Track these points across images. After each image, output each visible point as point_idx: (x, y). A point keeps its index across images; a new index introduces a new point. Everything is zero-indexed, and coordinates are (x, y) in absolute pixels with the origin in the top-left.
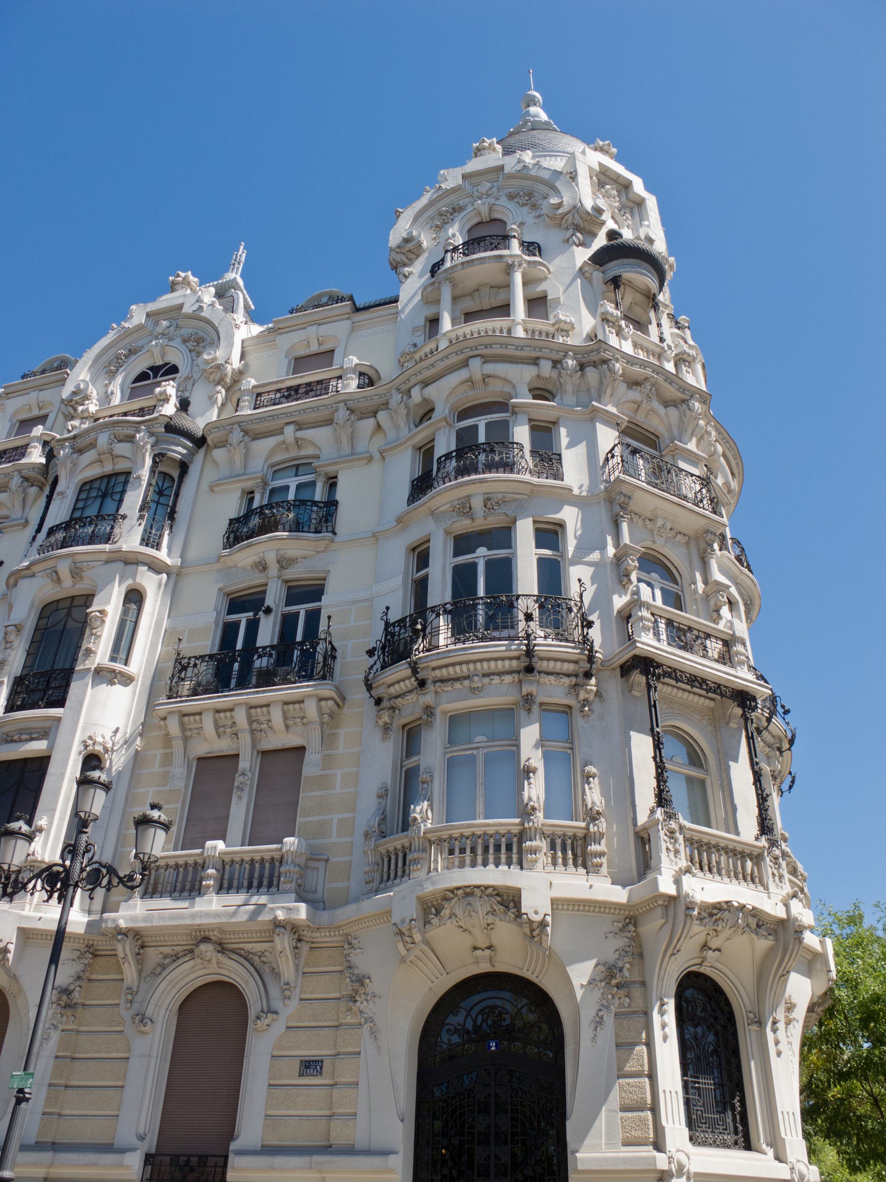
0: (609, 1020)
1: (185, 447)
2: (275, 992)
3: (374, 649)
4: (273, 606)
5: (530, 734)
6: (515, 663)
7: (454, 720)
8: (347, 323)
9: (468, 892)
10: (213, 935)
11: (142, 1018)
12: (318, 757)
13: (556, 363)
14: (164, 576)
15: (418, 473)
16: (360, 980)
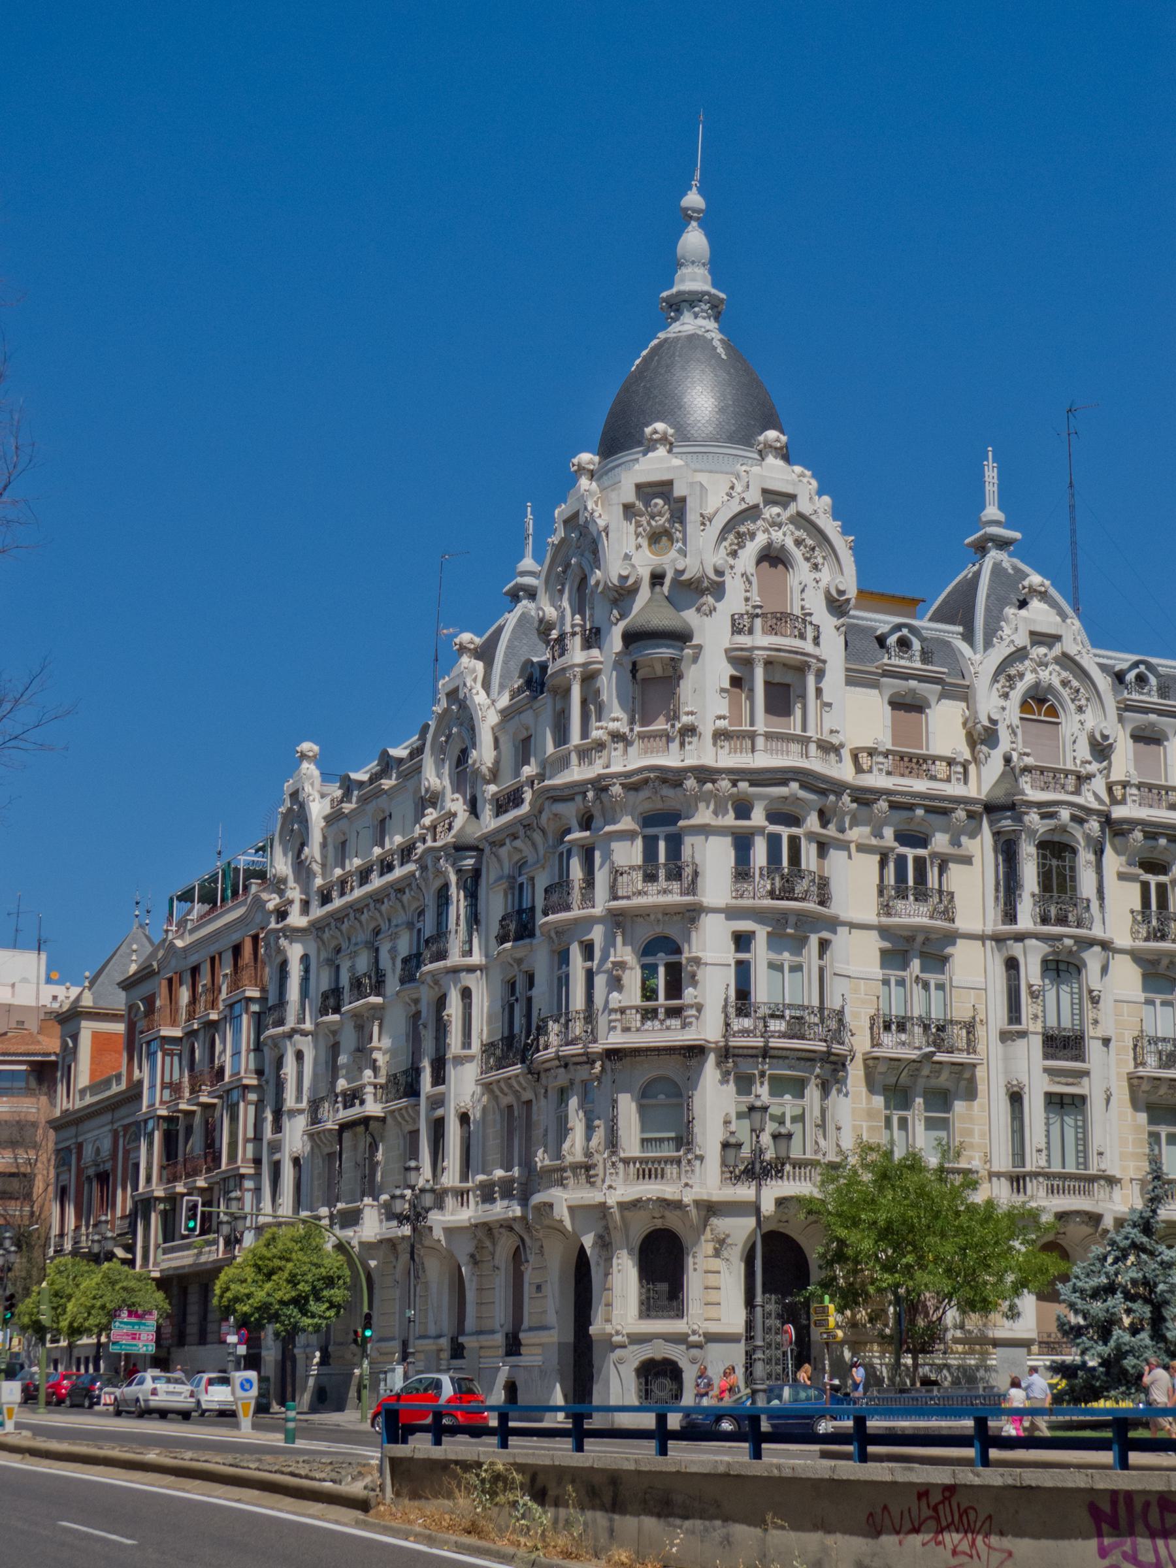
1: (471, 857)
2: (528, 1251)
5: (573, 1102)
8: (530, 712)
14: (478, 972)
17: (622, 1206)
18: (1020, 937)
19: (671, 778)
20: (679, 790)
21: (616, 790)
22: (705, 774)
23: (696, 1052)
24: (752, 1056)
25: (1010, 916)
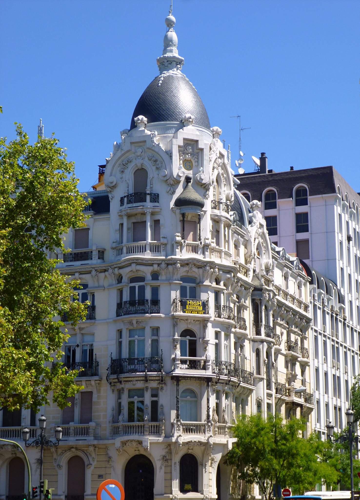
0: (163, 468)
2: (91, 459)
3: (108, 368)
4: (79, 344)
6: (143, 378)
7: (129, 391)
9: (132, 441)
10: (74, 447)
11: (59, 466)
12: (96, 396)
13: (159, 265)
15: (119, 302)
16: (110, 458)
17: (185, 444)
18: (262, 341)
19: (202, 265)
20: (201, 270)
21: (179, 265)
22: (212, 265)
23: (208, 380)
24: (222, 383)
25: (258, 333)
